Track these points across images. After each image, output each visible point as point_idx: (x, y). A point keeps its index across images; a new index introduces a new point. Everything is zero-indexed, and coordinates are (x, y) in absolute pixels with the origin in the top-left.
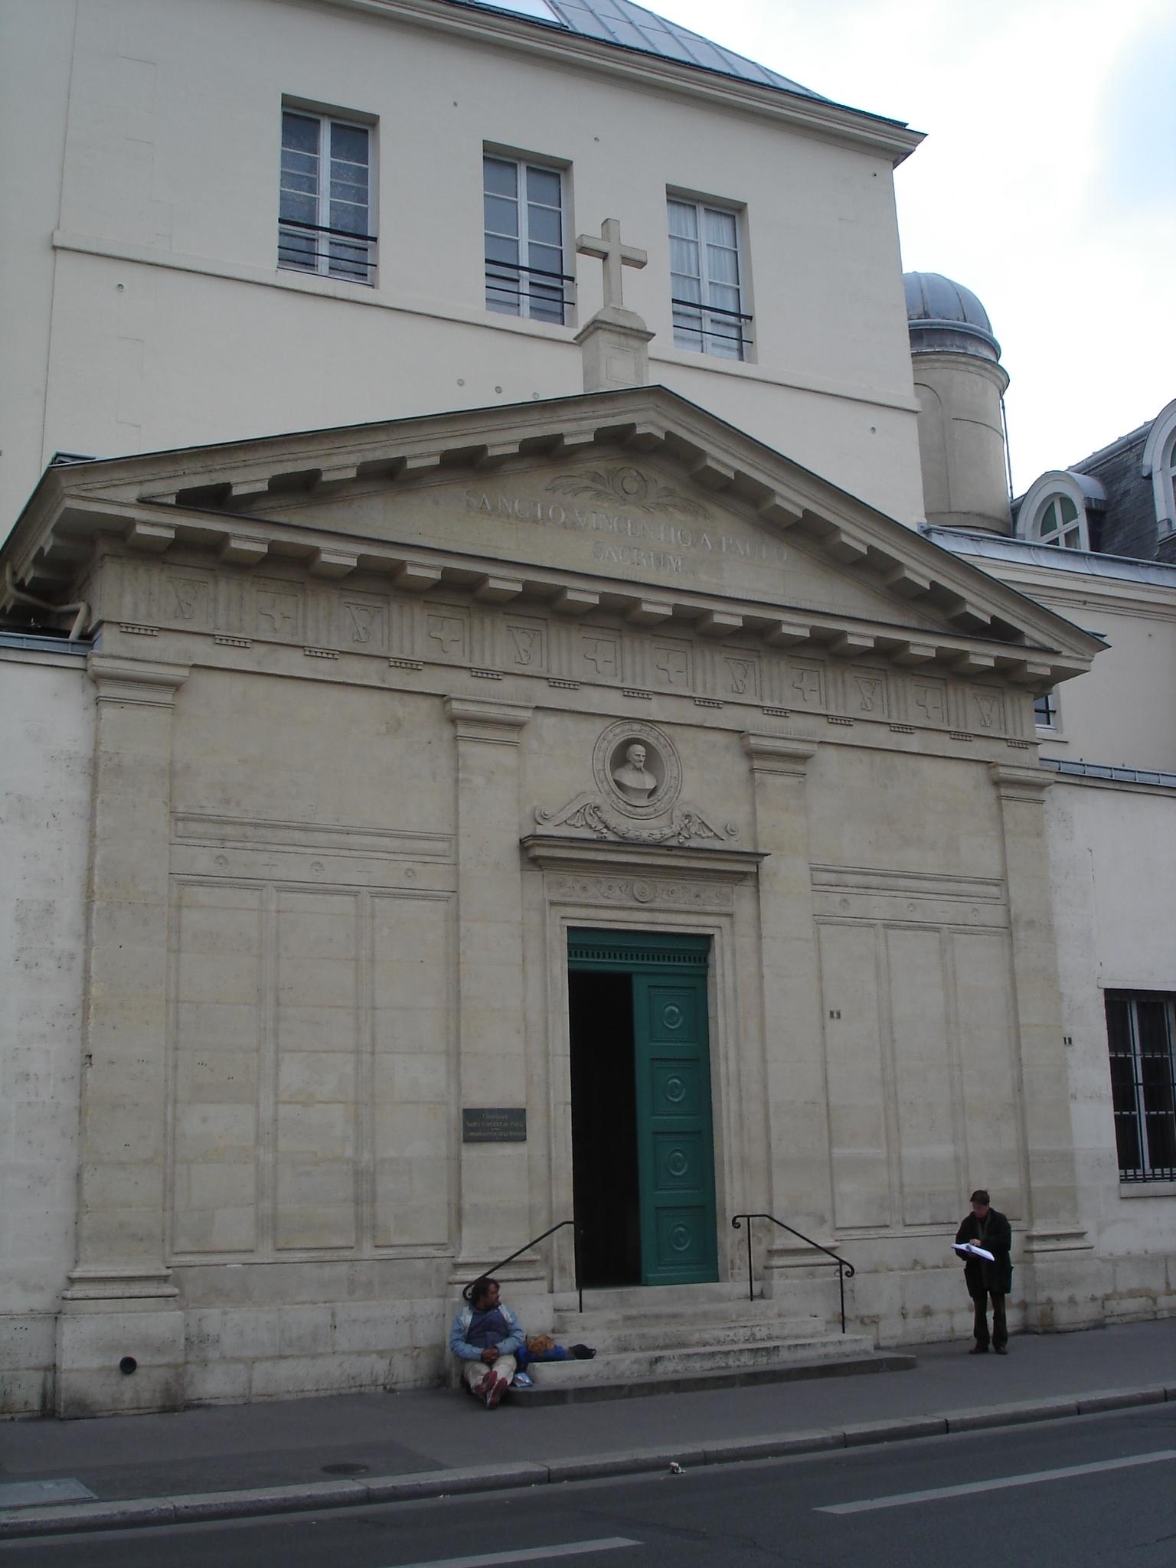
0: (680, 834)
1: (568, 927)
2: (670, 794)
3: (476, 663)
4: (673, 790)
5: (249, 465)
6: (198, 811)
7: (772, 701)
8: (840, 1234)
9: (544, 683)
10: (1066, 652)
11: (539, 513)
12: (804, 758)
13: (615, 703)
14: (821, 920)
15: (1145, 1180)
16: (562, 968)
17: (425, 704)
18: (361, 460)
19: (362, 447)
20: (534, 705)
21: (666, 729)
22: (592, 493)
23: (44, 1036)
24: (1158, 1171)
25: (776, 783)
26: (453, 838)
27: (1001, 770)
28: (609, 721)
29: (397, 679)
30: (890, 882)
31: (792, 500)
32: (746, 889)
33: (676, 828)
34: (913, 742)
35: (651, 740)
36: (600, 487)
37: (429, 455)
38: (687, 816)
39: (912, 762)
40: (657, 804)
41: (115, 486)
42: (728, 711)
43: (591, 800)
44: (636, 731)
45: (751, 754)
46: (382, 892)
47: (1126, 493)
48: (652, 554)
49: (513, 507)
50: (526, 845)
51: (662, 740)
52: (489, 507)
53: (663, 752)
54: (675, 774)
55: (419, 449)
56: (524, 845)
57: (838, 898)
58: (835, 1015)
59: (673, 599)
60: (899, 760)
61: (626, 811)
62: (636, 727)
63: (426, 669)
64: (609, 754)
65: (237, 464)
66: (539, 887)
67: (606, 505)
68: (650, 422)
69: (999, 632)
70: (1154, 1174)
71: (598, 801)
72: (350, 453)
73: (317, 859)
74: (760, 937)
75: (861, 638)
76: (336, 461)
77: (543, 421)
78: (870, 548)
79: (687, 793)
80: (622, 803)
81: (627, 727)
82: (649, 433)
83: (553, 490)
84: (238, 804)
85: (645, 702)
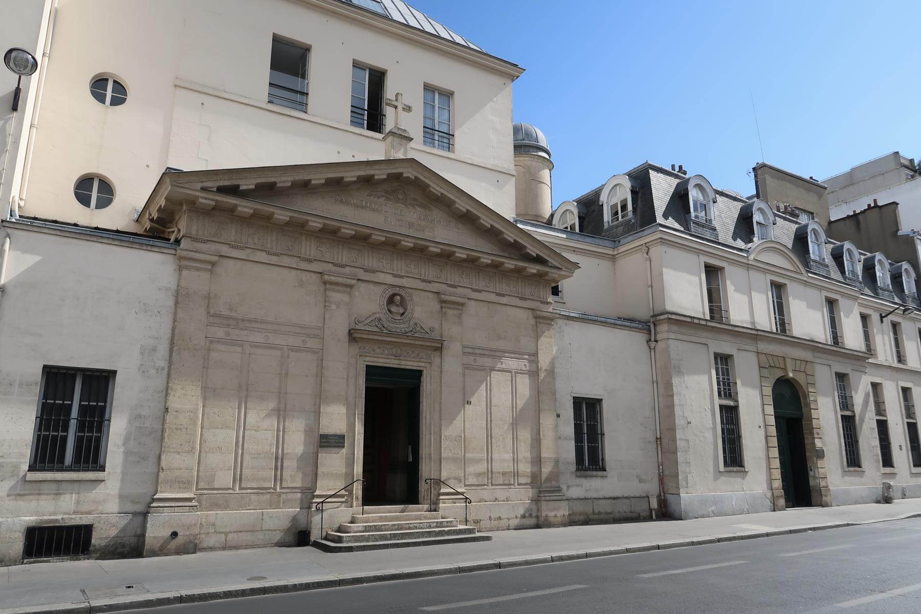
0: (412, 331)
1: (366, 365)
3: (335, 261)
6: (219, 313)
7: (451, 282)
8: (468, 488)
9: (362, 270)
12: (462, 304)
13: (389, 279)
14: (466, 367)
15: (586, 470)
17: (314, 276)
20: (358, 278)
21: (409, 290)
23: (149, 400)
24: (591, 467)
25: (451, 312)
27: (538, 312)
28: (387, 286)
30: (493, 353)
32: (438, 353)
33: (411, 329)
34: (504, 300)
35: (403, 294)
38: (415, 324)
39: (504, 308)
43: (377, 315)
44: (397, 290)
45: (442, 302)
46: (293, 349)
47: (593, 211)
50: (351, 332)
53: (408, 299)
54: (412, 308)
56: (350, 333)
57: (472, 358)
59: (413, 241)
60: (499, 307)
62: (397, 289)
64: (386, 299)
69: (539, 260)
70: (589, 468)
71: (381, 316)
74: (441, 372)
75: (486, 260)
78: (491, 225)
79: (416, 315)
81: (394, 289)
84: (236, 311)
85: (402, 279)
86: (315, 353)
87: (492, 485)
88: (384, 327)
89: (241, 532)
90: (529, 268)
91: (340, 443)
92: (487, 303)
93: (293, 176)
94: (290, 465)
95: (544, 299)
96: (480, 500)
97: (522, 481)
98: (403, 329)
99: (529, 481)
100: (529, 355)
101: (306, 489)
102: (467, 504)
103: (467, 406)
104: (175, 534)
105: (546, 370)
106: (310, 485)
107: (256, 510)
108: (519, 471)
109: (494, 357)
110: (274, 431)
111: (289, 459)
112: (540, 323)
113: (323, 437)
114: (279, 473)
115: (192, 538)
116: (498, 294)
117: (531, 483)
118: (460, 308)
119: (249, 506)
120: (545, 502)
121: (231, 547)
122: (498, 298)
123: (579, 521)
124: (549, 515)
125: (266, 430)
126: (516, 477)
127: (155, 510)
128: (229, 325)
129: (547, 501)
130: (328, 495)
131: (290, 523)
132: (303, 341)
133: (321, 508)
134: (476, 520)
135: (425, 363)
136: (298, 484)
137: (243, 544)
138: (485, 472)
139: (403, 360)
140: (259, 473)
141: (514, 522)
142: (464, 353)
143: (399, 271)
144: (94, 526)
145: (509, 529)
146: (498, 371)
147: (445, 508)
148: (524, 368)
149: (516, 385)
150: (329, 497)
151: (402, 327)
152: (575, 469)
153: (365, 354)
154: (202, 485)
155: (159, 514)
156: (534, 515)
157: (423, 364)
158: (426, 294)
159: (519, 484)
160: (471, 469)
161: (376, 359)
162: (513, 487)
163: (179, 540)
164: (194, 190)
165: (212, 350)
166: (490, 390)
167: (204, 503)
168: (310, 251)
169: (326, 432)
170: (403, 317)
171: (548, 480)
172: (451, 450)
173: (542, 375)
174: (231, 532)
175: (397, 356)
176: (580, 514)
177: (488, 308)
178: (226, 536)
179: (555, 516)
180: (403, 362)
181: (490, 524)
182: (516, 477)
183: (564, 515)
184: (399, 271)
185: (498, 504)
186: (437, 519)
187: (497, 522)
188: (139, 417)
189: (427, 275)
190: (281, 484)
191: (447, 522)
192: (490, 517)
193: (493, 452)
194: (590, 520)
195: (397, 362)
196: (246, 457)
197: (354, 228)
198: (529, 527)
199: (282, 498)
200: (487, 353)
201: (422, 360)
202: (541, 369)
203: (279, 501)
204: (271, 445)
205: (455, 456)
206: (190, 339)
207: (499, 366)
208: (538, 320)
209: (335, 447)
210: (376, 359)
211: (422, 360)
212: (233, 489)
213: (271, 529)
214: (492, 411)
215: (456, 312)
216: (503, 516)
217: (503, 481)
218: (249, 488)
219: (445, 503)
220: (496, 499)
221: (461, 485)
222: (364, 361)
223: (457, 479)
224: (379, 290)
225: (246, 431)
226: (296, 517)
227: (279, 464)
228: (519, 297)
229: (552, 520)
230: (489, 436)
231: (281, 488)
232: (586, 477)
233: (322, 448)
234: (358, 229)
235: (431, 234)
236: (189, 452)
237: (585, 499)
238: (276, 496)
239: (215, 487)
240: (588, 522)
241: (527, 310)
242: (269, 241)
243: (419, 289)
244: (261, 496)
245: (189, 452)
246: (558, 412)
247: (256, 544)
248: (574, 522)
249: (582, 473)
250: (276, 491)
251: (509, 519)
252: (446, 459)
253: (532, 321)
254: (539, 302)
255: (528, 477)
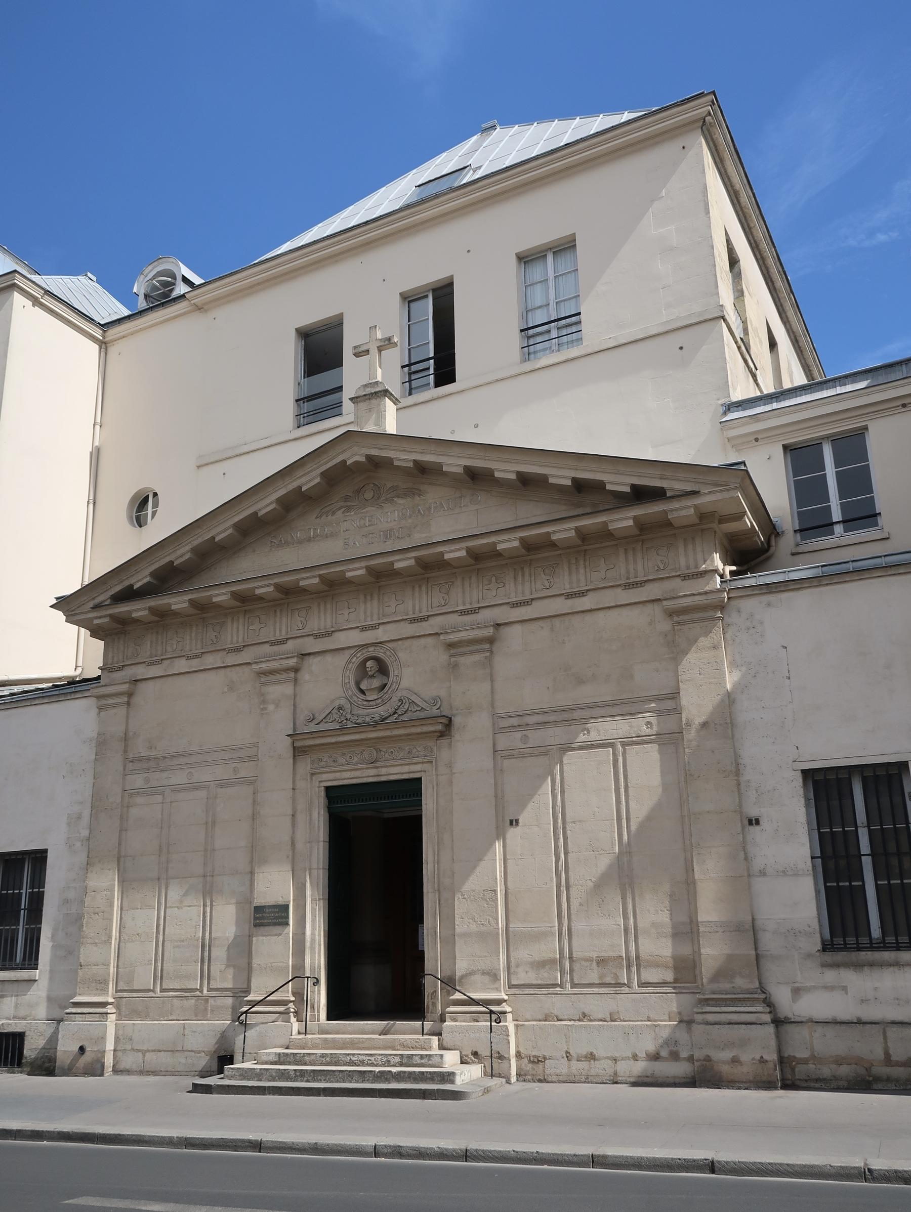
0: (395, 713)
2: (393, 687)
4: (395, 684)
5: (139, 572)
9: (311, 638)
10: (704, 491)
11: (312, 534)
13: (355, 638)
15: (859, 949)
16: (319, 814)
18: (191, 547)
19: (189, 541)
21: (390, 645)
22: (344, 509)
26: (256, 745)
29: (232, 659)
30: (565, 716)
31: (454, 464)
32: (444, 742)
33: (391, 711)
34: (585, 603)
35: (381, 655)
36: (349, 504)
37: (225, 530)
38: (400, 700)
39: (588, 617)
40: (384, 696)
41: (83, 604)
42: (432, 621)
43: (337, 704)
46: (223, 784)
48: (382, 533)
49: (297, 536)
51: (388, 653)
52: (283, 542)
53: (388, 661)
54: (396, 673)
55: (219, 529)
57: (519, 735)
58: (514, 823)
59: (363, 564)
60: (575, 620)
61: (363, 705)
62: (371, 649)
63: (246, 649)
65: (134, 573)
66: (305, 766)
67: (353, 513)
68: (355, 455)
70: (884, 941)
71: (343, 702)
72: (185, 545)
73: (190, 770)
76: (179, 553)
77: (285, 484)
79: (405, 683)
80: (361, 700)
81: (364, 651)
82: (356, 461)
83: (321, 516)
86: (251, 783)
87: (574, 985)
88: (346, 719)
89: (159, 1051)
90: (612, 521)
91: (282, 917)
92: (549, 620)
93: (190, 542)
94: (219, 954)
95: (688, 568)
96: (547, 1016)
97: (651, 975)
98: (376, 715)
99: (669, 976)
100: (657, 699)
101: (240, 991)
102: (494, 1024)
103: (512, 832)
104: (82, 1049)
105: (705, 725)
106: (245, 986)
107: (179, 1020)
108: (642, 954)
109: (569, 722)
110: (200, 906)
111: (218, 946)
112: (679, 623)
113: (259, 909)
114: (206, 967)
115: (100, 1055)
116: (569, 596)
117: (676, 981)
118: (487, 646)
119: (171, 1014)
120: (703, 1026)
121: (148, 1072)
122: (570, 602)
123: (835, 1078)
124: (714, 1059)
125: (189, 906)
126: (634, 969)
127: (68, 1017)
128: (148, 769)
129: (708, 1023)
130: (255, 1001)
131: (216, 1043)
132: (235, 770)
133: (244, 1022)
134: (535, 1056)
135: (423, 763)
136: (229, 985)
137: (162, 1069)
138: (556, 959)
139: (382, 767)
140: (183, 967)
141: (639, 1067)
142: (497, 731)
143: (369, 619)
144: (26, 1034)
145: (616, 1083)
146: (581, 748)
147: (452, 1030)
148: (645, 730)
149: (625, 771)
150: (255, 1005)
151: (383, 711)
152: (819, 946)
153: (318, 771)
154: (122, 986)
155: (70, 1023)
156: (684, 1054)
157: (418, 767)
158: (423, 641)
159: (642, 984)
160: (523, 954)
161: (338, 775)
162: (626, 989)
163: (87, 1057)
164: (86, 613)
165: (132, 806)
166: (563, 792)
167: (123, 1008)
168: (238, 637)
169: (263, 901)
170: (382, 693)
171: (719, 975)
172: (473, 919)
173: (691, 735)
174: (148, 1051)
175: (373, 762)
176: (839, 1061)
177: (552, 630)
178: (144, 1056)
179: (735, 1061)
180: (384, 771)
181: (569, 1067)
182: (634, 969)
183: (762, 1061)
184: (369, 619)
185: (585, 1027)
186: (426, 1050)
187: (584, 1065)
188: (66, 901)
189: (417, 608)
190: (209, 983)
191: (422, 1057)
192: (567, 1052)
193: (573, 917)
194: (877, 1079)
195: (372, 772)
196: (167, 944)
197: (270, 582)
198: (672, 1081)
199: (209, 1004)
200: (552, 718)
201: (416, 760)
202: (688, 725)
203: (206, 1009)
204: (196, 928)
205: (483, 929)
206: (107, 796)
207: (582, 738)
208: (676, 618)
209: (275, 924)
210: (357, 774)
211: (416, 760)
212: (153, 991)
213: (194, 1049)
214: (568, 832)
215: (477, 657)
216: (600, 1052)
217: (600, 978)
218: (171, 989)
219: (455, 1020)
220: (584, 1015)
221: (496, 985)
222: (320, 782)
223: (488, 974)
224: (340, 660)
225: (167, 909)
226: (225, 1033)
227: (206, 954)
228: (619, 585)
229: (725, 1069)
230: (564, 883)
231: (209, 990)
232: (858, 966)
233: (257, 927)
234: (277, 580)
235: (424, 535)
236: (105, 942)
237: (860, 1022)
238: (202, 1002)
239: (135, 988)
240: (869, 1082)
241: (650, 606)
242: (188, 642)
243: (408, 638)
244: (185, 1001)
245: (105, 942)
246: (753, 813)
247: (177, 1070)
248: (818, 1080)
249: (840, 956)
250: (202, 993)
251: (615, 1060)
252: (464, 935)
253: (665, 625)
254: (678, 580)
255: (667, 967)
